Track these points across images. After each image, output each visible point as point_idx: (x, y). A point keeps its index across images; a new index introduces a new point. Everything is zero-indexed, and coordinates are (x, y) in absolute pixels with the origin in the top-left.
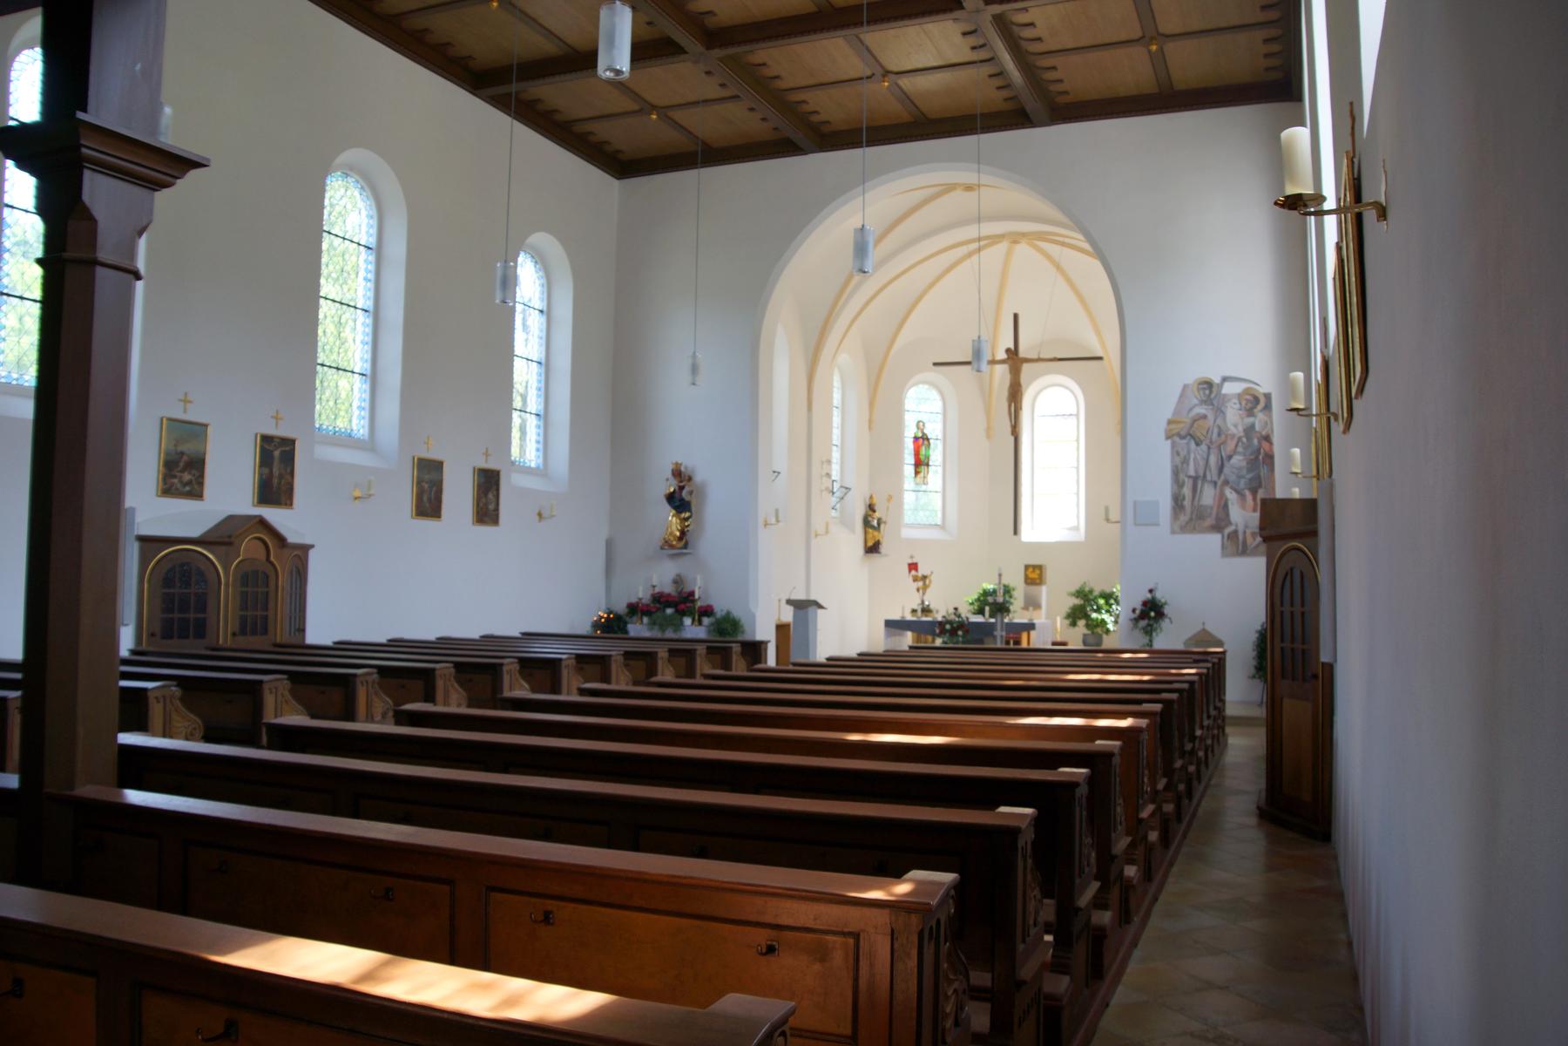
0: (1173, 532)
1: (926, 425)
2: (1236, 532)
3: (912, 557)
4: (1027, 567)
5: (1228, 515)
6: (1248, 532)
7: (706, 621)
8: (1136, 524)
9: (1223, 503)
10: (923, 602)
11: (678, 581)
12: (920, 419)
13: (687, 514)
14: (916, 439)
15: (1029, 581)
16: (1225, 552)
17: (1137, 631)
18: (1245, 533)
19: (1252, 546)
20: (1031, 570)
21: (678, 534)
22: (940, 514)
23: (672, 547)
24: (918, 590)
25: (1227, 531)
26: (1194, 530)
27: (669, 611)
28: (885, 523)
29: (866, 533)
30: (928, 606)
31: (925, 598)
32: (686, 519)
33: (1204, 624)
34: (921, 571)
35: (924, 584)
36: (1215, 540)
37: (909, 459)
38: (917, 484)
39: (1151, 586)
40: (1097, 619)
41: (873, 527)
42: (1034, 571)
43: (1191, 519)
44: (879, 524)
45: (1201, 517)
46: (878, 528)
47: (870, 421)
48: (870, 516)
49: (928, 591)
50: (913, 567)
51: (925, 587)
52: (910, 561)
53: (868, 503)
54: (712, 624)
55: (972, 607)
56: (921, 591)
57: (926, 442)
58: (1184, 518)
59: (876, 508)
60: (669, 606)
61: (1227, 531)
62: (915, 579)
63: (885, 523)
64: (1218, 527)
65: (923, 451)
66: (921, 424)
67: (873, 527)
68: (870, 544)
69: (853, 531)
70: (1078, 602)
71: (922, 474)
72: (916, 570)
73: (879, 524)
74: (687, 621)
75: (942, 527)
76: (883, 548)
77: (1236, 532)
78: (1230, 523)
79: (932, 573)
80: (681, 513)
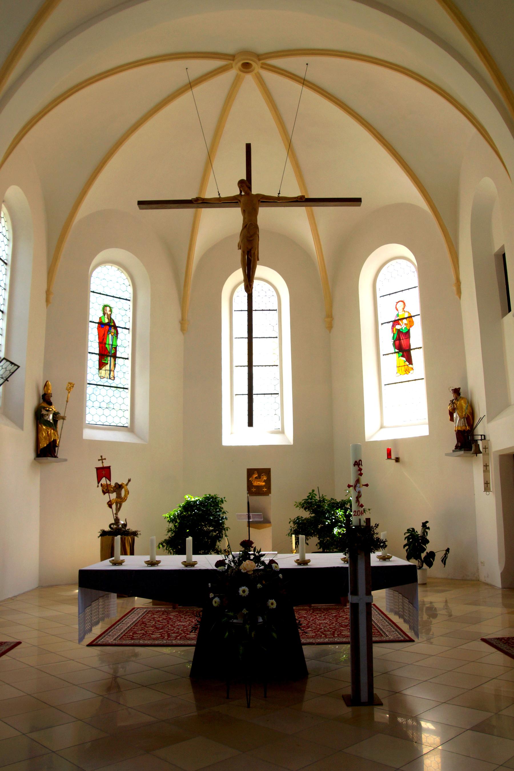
1: (113, 310)
3: (102, 459)
4: (250, 472)
10: (117, 520)
12: (106, 304)
14: (101, 324)
20: (256, 476)
22: (128, 414)
24: (110, 505)
28: (63, 418)
29: (38, 431)
30: (125, 525)
31: (120, 515)
34: (116, 478)
35: (119, 496)
37: (94, 346)
38: (102, 378)
40: (339, 533)
41: (47, 423)
42: (259, 478)
44: (55, 420)
46: (54, 425)
47: (48, 293)
48: (44, 408)
49: (124, 504)
51: (120, 502)
52: (100, 465)
53: (42, 393)
55: (171, 525)
56: (114, 506)
57: (113, 330)
59: (52, 400)
62: (106, 490)
63: (63, 418)
65: (109, 339)
66: (108, 309)
67: (47, 423)
68: (44, 444)
69: (21, 426)
70: (306, 515)
71: (107, 367)
73: (55, 420)
75: (131, 429)
76: (61, 452)
79: (129, 480)
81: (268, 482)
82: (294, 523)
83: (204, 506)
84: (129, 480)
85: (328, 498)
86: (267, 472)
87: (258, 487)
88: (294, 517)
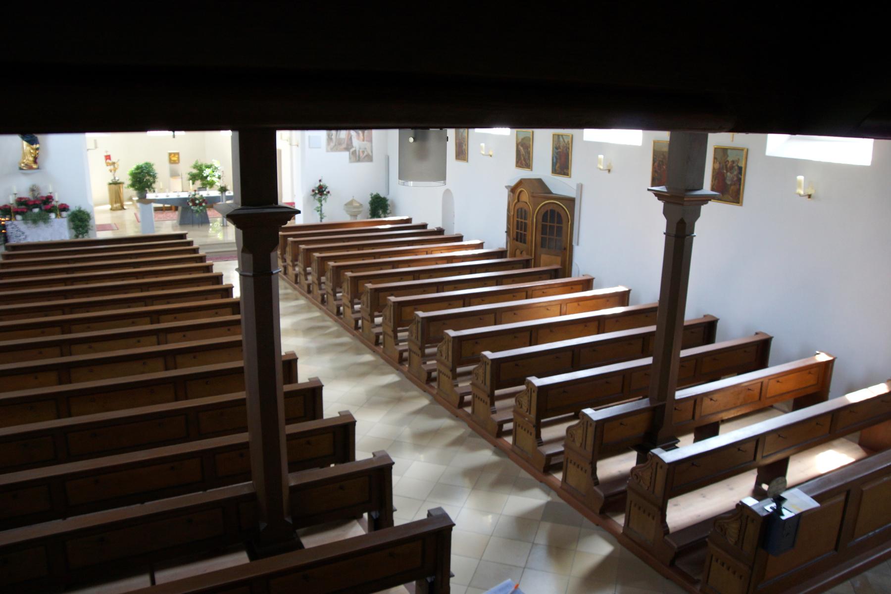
0: (327, 151)
2: (355, 151)
4: (170, 154)
5: (352, 143)
6: (361, 150)
7: (64, 214)
8: (309, 148)
9: (349, 137)
11: (33, 190)
13: (38, 146)
15: (172, 162)
16: (351, 161)
17: (316, 201)
18: (359, 151)
19: (363, 157)
20: (173, 155)
21: (31, 159)
23: (31, 168)
24: (111, 171)
25: (352, 150)
26: (337, 150)
27: (36, 210)
30: (118, 180)
32: (37, 149)
33: (353, 197)
34: (113, 159)
36: (346, 155)
39: (320, 178)
42: (174, 156)
43: (335, 145)
45: (340, 144)
49: (117, 171)
50: (108, 157)
51: (115, 170)
52: (106, 154)
54: (69, 216)
56: (113, 171)
58: (332, 144)
60: (36, 207)
61: (352, 150)
62: (108, 164)
64: (347, 149)
70: (195, 171)
72: (110, 159)
74: (53, 215)
77: (355, 151)
78: (352, 147)
80: (33, 144)
81: (178, 158)
82: (189, 174)
83: (147, 168)
84: (118, 160)
85: (204, 163)
86: (178, 154)
87: (174, 161)
88: (188, 172)
